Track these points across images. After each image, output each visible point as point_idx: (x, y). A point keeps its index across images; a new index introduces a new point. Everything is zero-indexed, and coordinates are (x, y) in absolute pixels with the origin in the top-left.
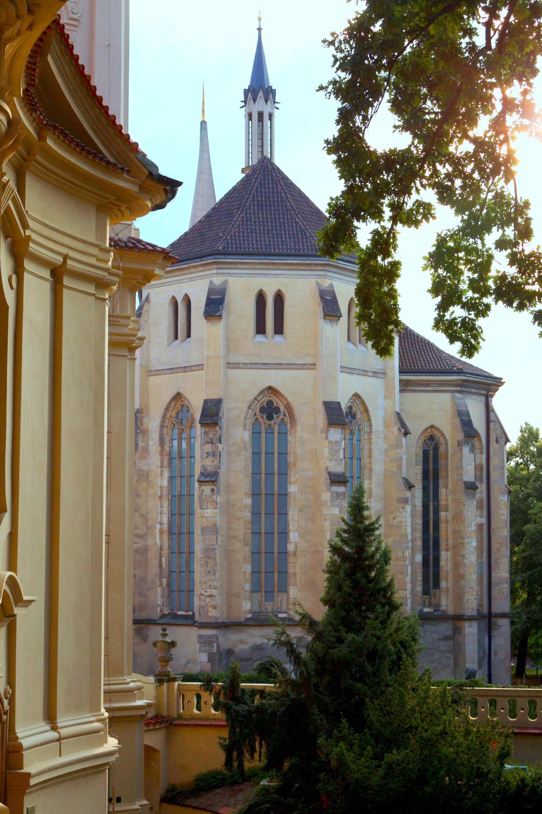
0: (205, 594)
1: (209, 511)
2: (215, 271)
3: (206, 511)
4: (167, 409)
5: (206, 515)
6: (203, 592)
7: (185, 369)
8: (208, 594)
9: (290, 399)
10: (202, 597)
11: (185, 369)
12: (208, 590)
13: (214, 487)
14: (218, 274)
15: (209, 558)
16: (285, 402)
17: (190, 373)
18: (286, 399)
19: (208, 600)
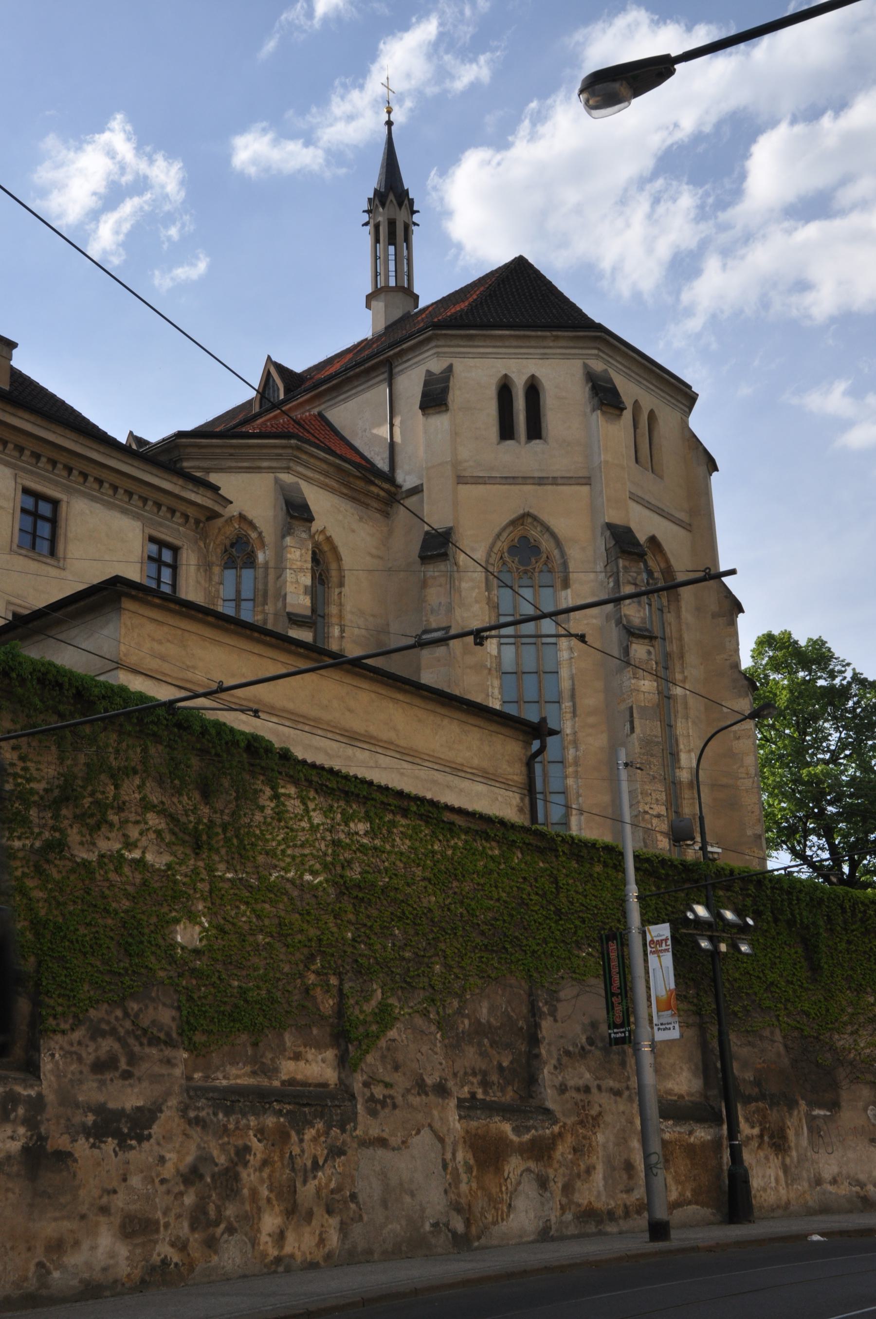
0: (651, 812)
1: (646, 682)
2: (595, 352)
3: (642, 682)
4: (499, 536)
5: (643, 689)
6: (647, 808)
7: (541, 481)
8: (655, 813)
9: (673, 561)
10: (647, 817)
11: (541, 481)
12: (654, 806)
13: (651, 649)
14: (597, 356)
15: (652, 755)
16: (663, 565)
17: (550, 487)
18: (667, 561)
19: (655, 821)
